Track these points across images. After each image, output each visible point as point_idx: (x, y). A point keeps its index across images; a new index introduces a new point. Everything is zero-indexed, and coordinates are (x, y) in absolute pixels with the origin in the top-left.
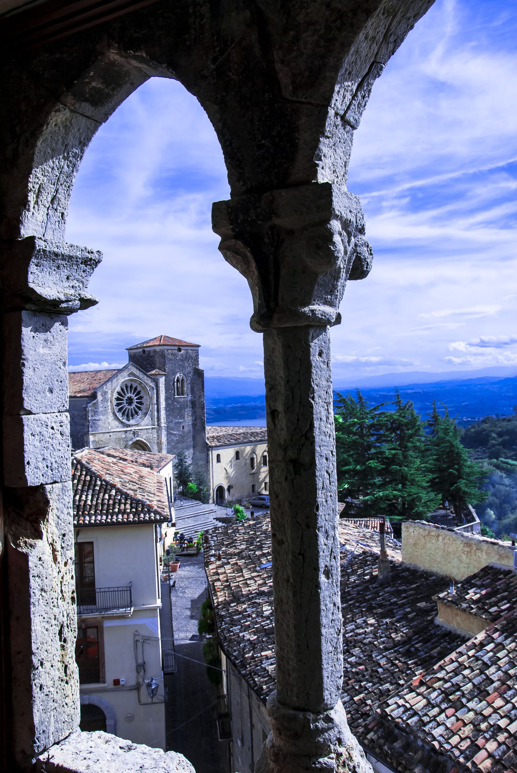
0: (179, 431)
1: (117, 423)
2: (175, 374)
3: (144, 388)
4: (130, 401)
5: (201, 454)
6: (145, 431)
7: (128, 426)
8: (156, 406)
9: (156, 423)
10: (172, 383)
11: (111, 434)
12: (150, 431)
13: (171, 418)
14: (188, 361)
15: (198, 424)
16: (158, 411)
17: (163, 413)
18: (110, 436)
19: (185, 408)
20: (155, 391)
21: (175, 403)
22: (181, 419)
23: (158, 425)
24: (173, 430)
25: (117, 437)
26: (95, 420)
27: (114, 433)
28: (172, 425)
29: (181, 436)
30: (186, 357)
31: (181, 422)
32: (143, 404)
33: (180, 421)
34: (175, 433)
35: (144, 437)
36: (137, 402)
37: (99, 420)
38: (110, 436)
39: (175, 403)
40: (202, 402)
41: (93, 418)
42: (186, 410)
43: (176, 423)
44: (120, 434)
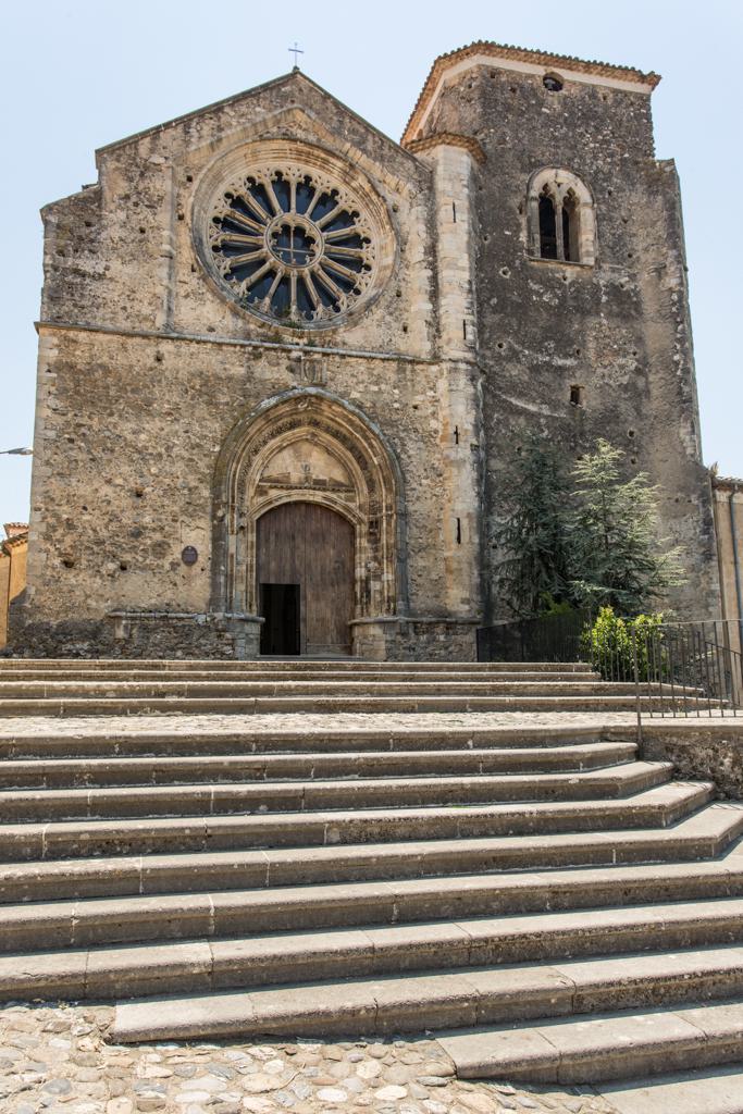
0: (555, 406)
2: (534, 166)
5: (672, 522)
11: (166, 347)
14: (598, 130)
15: (655, 392)
18: (159, 359)
19: (584, 313)
22: (567, 356)
24: (521, 395)
25: (197, 365)
26: (77, 272)
28: (514, 371)
29: (565, 427)
31: (561, 369)
32: (368, 268)
34: (532, 408)
35: (355, 395)
37: (101, 277)
38: (159, 359)
40: (671, 290)
41: (70, 262)
42: (592, 321)
43: (535, 369)
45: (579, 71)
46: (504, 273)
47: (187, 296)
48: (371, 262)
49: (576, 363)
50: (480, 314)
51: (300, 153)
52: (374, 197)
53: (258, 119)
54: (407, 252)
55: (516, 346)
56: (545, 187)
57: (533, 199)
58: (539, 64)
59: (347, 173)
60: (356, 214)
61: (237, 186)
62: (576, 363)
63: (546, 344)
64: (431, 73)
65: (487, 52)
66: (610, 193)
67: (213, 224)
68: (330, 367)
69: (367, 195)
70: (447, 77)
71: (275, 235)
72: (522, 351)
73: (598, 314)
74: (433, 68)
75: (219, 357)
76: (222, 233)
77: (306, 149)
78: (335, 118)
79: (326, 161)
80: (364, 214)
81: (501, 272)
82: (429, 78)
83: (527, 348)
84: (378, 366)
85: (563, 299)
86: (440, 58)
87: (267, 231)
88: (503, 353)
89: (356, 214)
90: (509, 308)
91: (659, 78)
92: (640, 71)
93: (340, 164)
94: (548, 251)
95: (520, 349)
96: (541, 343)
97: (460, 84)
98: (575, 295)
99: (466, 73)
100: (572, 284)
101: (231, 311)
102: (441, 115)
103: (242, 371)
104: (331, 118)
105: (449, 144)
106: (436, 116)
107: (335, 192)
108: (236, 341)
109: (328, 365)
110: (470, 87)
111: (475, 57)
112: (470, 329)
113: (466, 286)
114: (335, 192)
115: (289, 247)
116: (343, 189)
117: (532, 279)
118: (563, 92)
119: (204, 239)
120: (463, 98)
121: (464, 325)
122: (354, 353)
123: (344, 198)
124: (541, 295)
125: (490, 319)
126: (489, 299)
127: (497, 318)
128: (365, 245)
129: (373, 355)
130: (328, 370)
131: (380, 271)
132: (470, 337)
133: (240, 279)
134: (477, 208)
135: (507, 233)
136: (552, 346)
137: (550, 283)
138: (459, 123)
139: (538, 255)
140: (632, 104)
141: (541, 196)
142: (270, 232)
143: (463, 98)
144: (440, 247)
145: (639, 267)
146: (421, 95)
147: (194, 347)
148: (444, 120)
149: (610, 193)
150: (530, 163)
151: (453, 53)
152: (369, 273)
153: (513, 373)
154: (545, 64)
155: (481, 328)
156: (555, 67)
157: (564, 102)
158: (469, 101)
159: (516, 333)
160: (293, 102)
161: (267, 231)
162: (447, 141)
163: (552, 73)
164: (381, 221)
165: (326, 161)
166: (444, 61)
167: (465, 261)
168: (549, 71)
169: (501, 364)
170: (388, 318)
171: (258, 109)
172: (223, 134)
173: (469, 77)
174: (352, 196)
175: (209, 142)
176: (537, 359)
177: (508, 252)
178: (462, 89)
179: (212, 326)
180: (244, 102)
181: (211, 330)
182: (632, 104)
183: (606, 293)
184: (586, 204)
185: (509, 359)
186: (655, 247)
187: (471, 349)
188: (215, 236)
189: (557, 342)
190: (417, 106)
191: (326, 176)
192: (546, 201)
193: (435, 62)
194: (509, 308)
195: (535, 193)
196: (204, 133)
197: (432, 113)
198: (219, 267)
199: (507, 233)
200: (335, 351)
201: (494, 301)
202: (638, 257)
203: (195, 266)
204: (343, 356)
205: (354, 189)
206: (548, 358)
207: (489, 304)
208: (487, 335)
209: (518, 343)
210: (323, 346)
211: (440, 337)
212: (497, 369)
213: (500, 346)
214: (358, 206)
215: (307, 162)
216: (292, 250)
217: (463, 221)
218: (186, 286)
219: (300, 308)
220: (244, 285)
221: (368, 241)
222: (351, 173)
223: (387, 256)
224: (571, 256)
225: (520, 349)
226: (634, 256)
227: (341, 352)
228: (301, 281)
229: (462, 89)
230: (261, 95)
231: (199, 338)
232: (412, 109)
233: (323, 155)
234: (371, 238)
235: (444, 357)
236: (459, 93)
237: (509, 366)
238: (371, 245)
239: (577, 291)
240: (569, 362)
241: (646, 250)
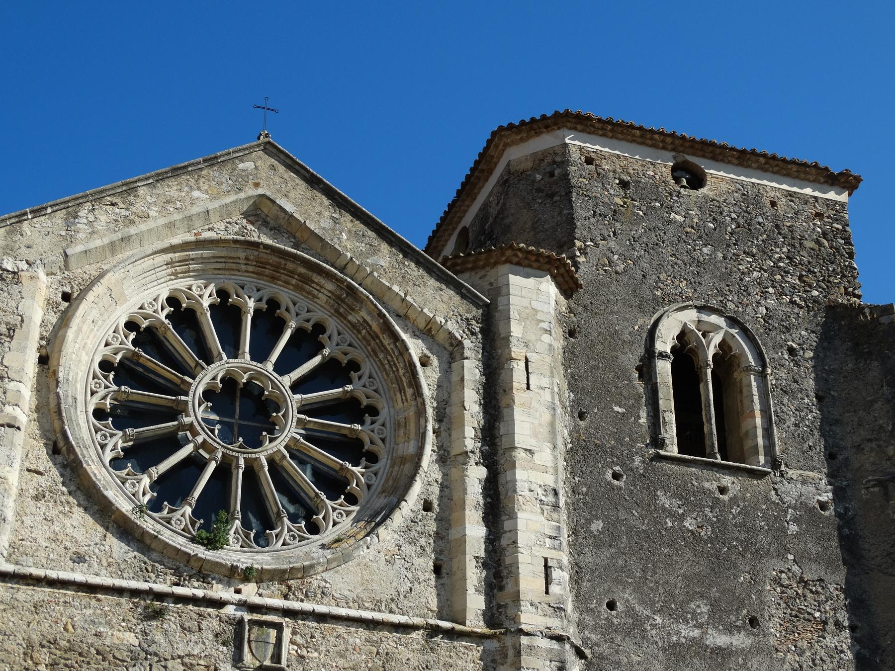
1: (80, 525)
3: (383, 341)
4: (245, 409)
6: (359, 636)
7: (203, 572)
8: (476, 474)
9: (476, 603)
10: (631, 358)
12: (408, 650)
13: (626, 597)
14: (766, 253)
16: (497, 507)
17: (537, 532)
19: (759, 555)
20: (472, 370)
21: (664, 501)
22: (731, 629)
23: (492, 617)
25: (43, 627)
27: (25, 593)
30: (747, 227)
33: (718, 639)
36: (260, 354)
39: (664, 501)
42: (772, 567)
44: (81, 611)
45: (729, 162)
46: (616, 476)
47: (36, 498)
48: (381, 450)
49: (748, 642)
50: (576, 549)
51: (262, 264)
52: (386, 341)
53: (195, 210)
54: (443, 434)
55: (638, 608)
56: (683, 336)
57: (662, 356)
58: (664, 148)
59: (343, 301)
60: (354, 366)
61: (149, 311)
62: (748, 642)
63: (693, 606)
64: (486, 149)
65: (579, 127)
66: (791, 351)
67: (98, 371)
68: (298, 639)
69: (375, 337)
70: (513, 158)
71: (208, 394)
72: (648, 618)
73: (784, 558)
74: (489, 142)
75: (89, 612)
76: (115, 388)
77: (273, 259)
78: (327, 214)
79: (307, 280)
80: (367, 367)
81: (609, 476)
82: (481, 155)
83: (660, 612)
84: (389, 640)
85: (721, 525)
86: (501, 128)
87: (199, 386)
88: (615, 621)
89: (354, 366)
90: (624, 539)
91: (858, 180)
92: (826, 169)
93: (330, 286)
94: (691, 439)
95: (648, 612)
96: (682, 605)
97: (535, 169)
98: (739, 520)
99: (545, 153)
100: (734, 500)
101: (119, 527)
102: (499, 213)
103: (131, 639)
104: (320, 213)
105: (518, 264)
106: (493, 211)
107: (319, 328)
108: (124, 583)
109: (294, 633)
110: (552, 174)
111: (560, 133)
112: (556, 574)
113: (551, 499)
114: (319, 328)
115: (233, 416)
116: (332, 325)
117: (666, 489)
118: (704, 190)
119: (80, 398)
120: (539, 190)
121: (547, 567)
122: (343, 612)
123: (335, 338)
124: (682, 518)
125: (588, 558)
126: (589, 522)
127: (604, 555)
128: (368, 419)
129: (377, 616)
130: (292, 642)
131: (392, 466)
132: (554, 588)
133: (144, 469)
134: (566, 366)
135: (617, 409)
136: (705, 609)
137: (692, 499)
138: (533, 228)
139: (673, 450)
140: (819, 215)
141: (673, 349)
142: (200, 390)
143: (539, 190)
144: (502, 432)
145: (849, 475)
146: (468, 177)
147: (43, 593)
148: (507, 221)
149: (791, 351)
150: (655, 298)
151: (523, 123)
152: (375, 467)
153: (635, 658)
154: (673, 150)
155: (578, 573)
156: (694, 154)
157: (712, 209)
158: (551, 196)
159: (637, 589)
160: (257, 185)
161: (199, 386)
162: (515, 260)
163: (686, 162)
164: (398, 380)
165: (307, 280)
166: (503, 136)
167: (545, 456)
168: (680, 159)
169: (612, 640)
170: (408, 549)
171: (196, 194)
172: (133, 230)
173: (549, 159)
174: (349, 337)
175: (106, 241)
176: (678, 633)
177: (620, 441)
178: (538, 177)
179: (82, 550)
180: (173, 182)
181: (79, 559)
182: (819, 215)
183: (796, 520)
184: (748, 369)
185: (627, 634)
186: (874, 445)
187: (559, 610)
188: (102, 392)
189: (714, 605)
190: (459, 193)
191: (303, 302)
192: (685, 354)
193: (494, 134)
194: (624, 539)
195: (665, 343)
196: (101, 225)
197: (485, 206)
198: (103, 447)
199: (617, 409)
200: (307, 606)
201: (597, 526)
202: (847, 459)
203: (61, 444)
204: (322, 618)
205: (353, 326)
206: (696, 633)
207: (588, 530)
208: (586, 585)
209: (641, 602)
210: (286, 597)
211: (501, 588)
212: (604, 649)
213: (611, 606)
214: (358, 354)
215: (273, 279)
216: (236, 420)
217: (543, 388)
218: (41, 480)
219: (246, 524)
220: (146, 481)
221: (374, 411)
222: (350, 301)
223: (408, 440)
224: (733, 446)
225: (648, 612)
226: (840, 457)
227: (321, 609)
228: (251, 474)
229: (538, 177)
230: (204, 172)
231: (53, 574)
232: (451, 196)
233: (302, 270)
234: (379, 406)
235: (507, 624)
236: (534, 181)
237: (627, 645)
238: (380, 419)
239: (744, 512)
240: (740, 640)
241: (859, 448)
